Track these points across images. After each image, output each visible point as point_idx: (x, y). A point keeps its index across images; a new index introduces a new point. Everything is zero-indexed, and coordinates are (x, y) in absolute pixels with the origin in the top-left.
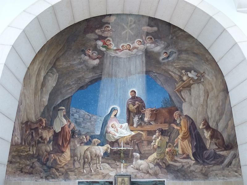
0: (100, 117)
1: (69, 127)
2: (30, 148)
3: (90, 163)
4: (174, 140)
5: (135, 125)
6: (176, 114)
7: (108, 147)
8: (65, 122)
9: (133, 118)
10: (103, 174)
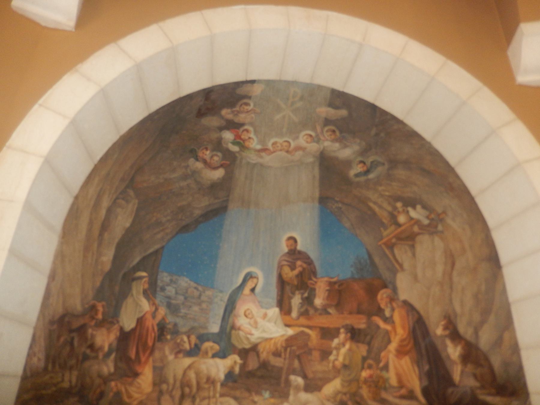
0: (221, 292)
1: (154, 316)
2: (63, 375)
4: (378, 354)
5: (294, 314)
7: (235, 362)
8: (146, 306)
9: (290, 298)
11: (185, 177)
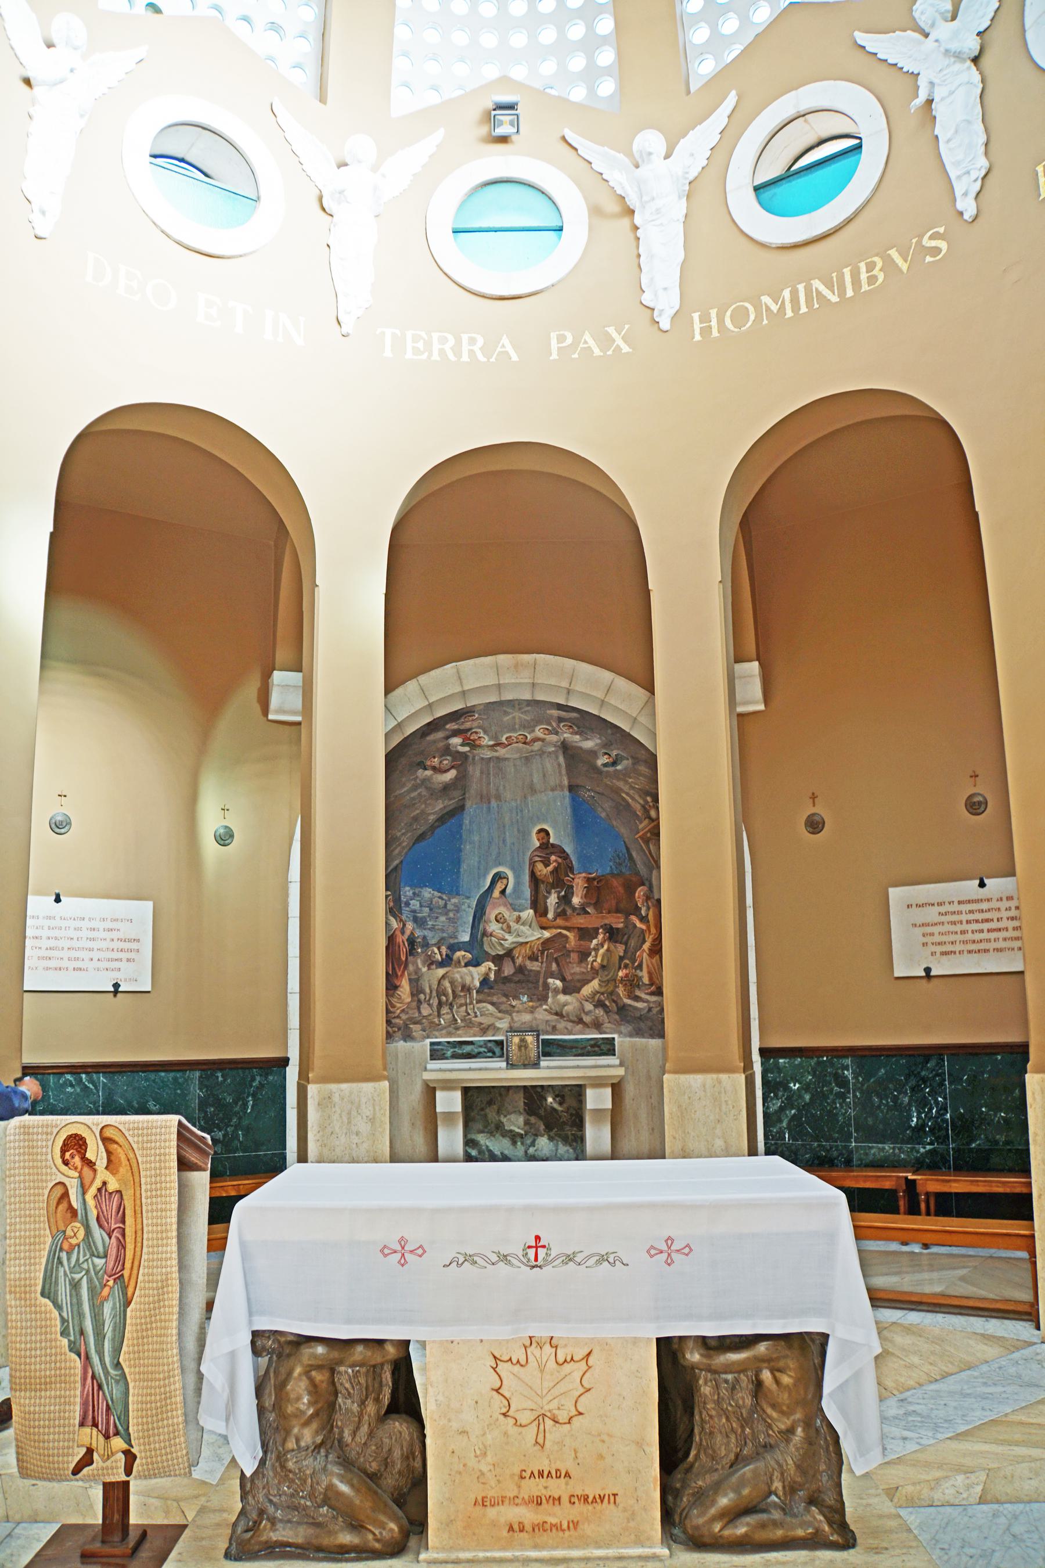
0: (468, 898)
1: (403, 933)
3: (451, 1004)
5: (550, 915)
6: (640, 892)
10: (482, 1026)
11: (415, 788)
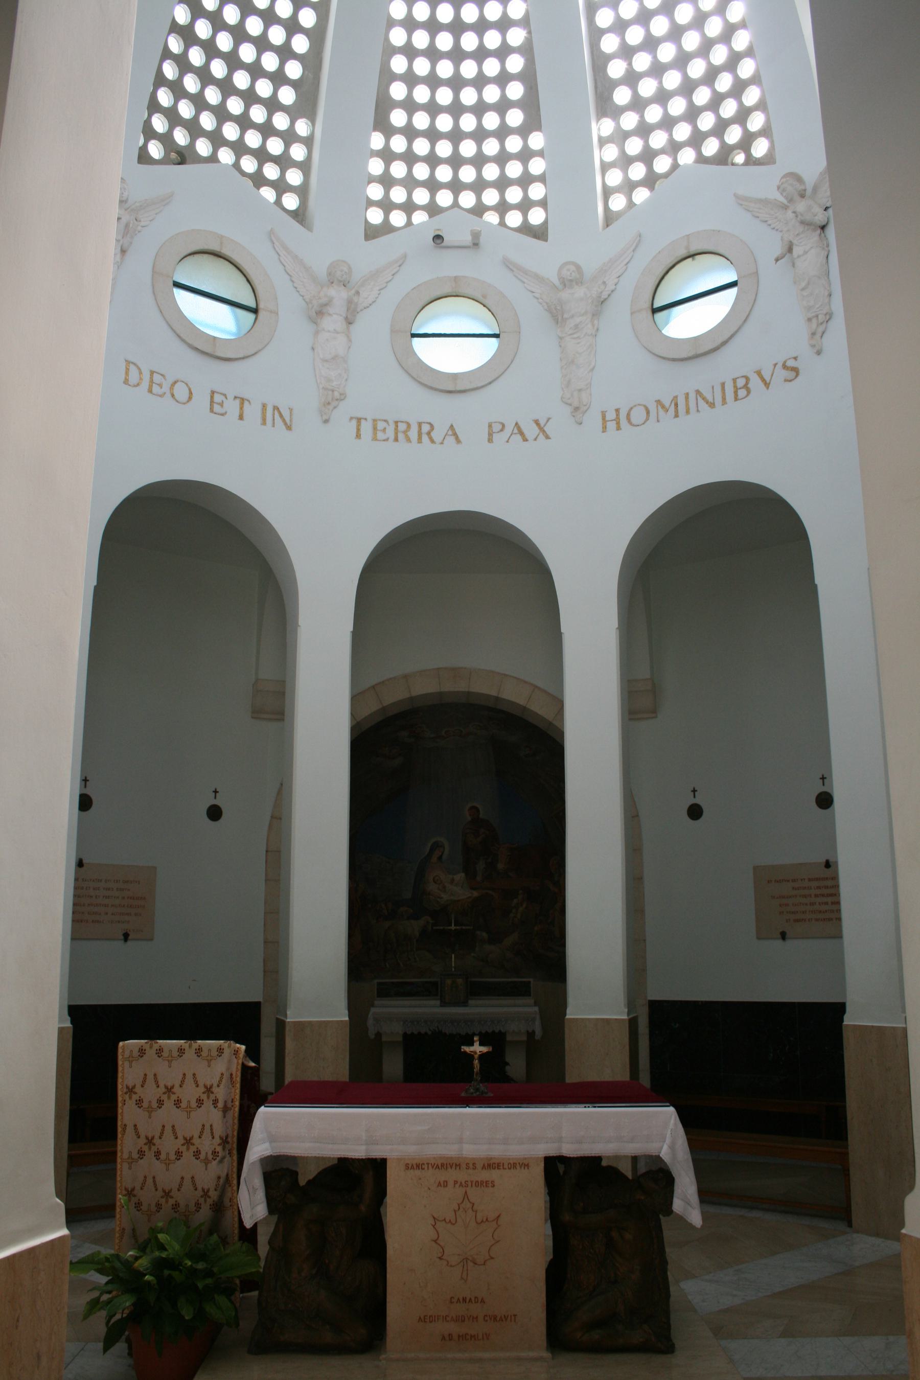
5: (479, 878)
